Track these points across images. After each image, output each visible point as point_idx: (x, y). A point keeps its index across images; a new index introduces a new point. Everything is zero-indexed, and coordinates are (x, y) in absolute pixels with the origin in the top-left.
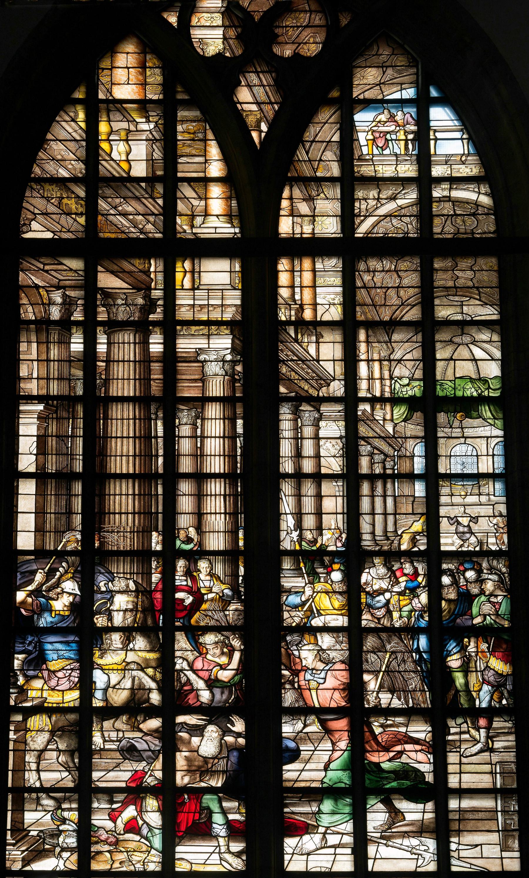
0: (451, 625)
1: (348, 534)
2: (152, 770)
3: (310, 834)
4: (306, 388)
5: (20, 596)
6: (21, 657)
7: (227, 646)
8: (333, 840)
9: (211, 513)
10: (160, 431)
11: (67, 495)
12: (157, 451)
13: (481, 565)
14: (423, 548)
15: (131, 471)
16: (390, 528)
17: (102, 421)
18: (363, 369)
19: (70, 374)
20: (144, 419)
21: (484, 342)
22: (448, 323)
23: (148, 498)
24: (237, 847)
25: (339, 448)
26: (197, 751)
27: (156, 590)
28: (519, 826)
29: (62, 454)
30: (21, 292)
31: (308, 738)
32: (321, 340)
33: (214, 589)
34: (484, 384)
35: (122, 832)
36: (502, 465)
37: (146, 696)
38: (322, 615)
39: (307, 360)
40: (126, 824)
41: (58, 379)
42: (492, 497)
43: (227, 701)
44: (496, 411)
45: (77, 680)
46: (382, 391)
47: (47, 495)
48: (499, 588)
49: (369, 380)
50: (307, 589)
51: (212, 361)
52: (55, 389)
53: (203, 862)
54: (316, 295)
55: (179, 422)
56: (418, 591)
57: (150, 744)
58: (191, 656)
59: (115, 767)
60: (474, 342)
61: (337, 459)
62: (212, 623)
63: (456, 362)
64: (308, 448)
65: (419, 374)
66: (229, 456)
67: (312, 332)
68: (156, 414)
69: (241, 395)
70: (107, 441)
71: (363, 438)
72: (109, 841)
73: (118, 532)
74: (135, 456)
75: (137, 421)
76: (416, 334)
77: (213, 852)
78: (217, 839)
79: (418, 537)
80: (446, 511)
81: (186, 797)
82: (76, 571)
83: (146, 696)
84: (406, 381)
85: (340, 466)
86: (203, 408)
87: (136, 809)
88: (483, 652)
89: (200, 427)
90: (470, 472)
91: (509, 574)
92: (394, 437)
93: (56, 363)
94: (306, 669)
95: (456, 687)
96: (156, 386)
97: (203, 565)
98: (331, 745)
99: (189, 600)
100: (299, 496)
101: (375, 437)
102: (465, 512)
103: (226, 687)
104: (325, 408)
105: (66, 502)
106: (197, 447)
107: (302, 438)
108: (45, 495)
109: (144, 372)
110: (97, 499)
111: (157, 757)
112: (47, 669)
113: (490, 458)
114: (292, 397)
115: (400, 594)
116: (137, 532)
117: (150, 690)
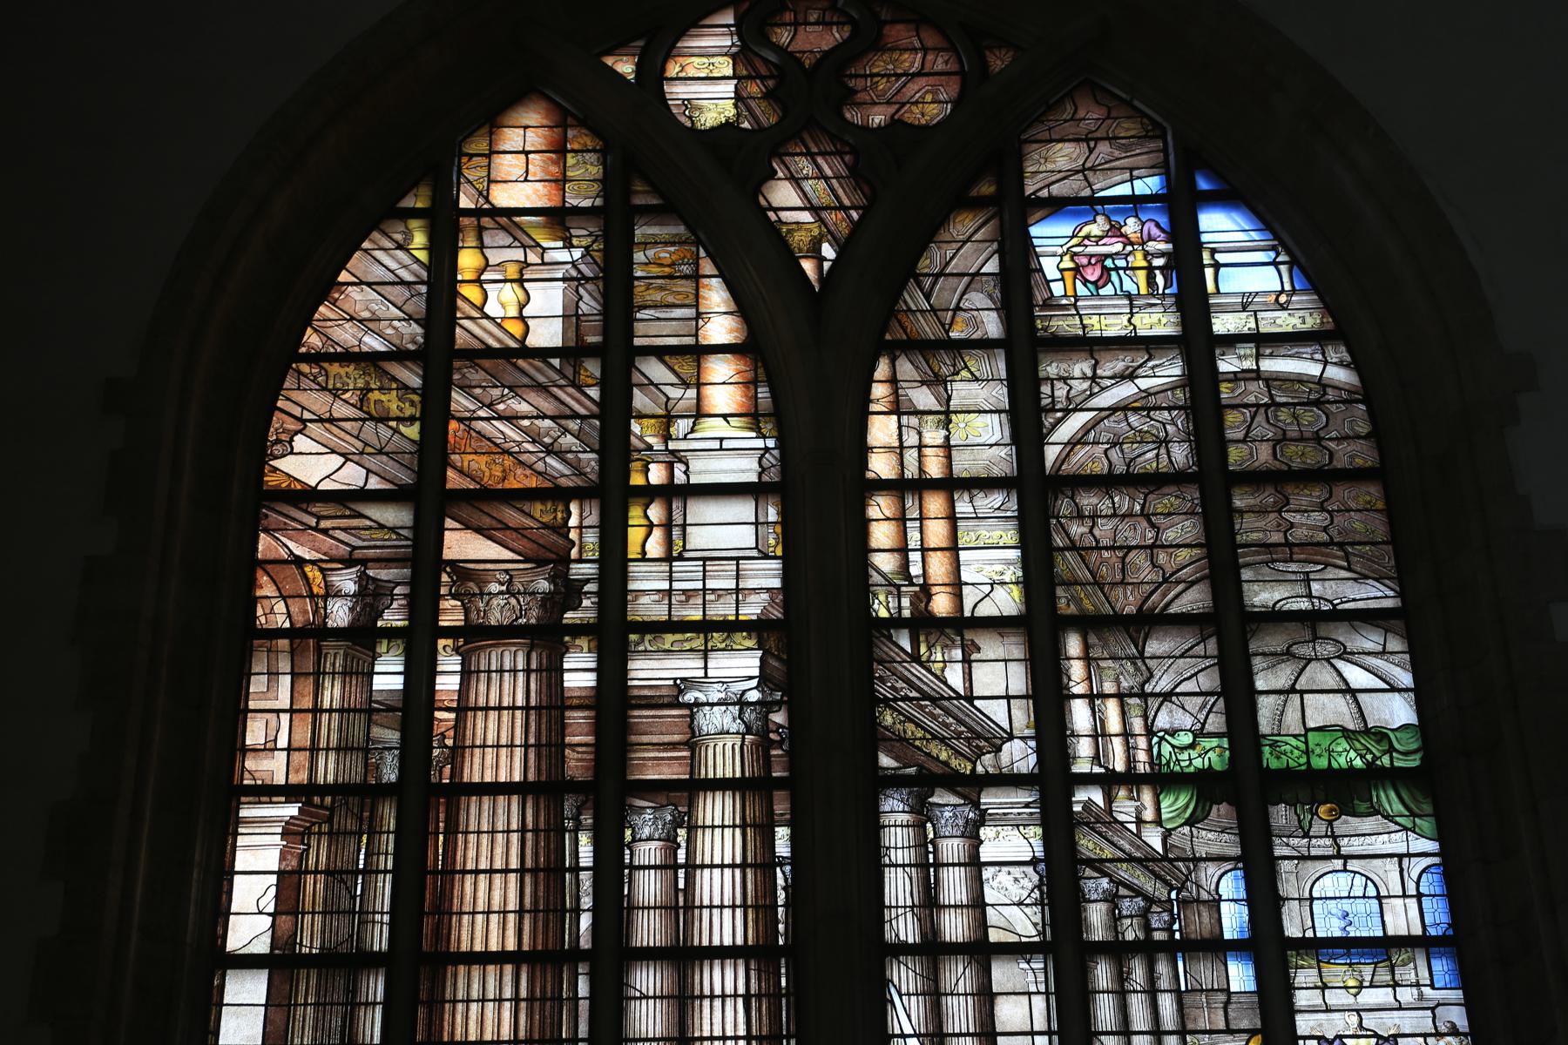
4: (943, 756)
10: (586, 855)
11: (346, 1004)
12: (578, 899)
15: (511, 945)
17: (441, 837)
18: (1080, 716)
19: (368, 739)
20: (547, 831)
21: (1369, 654)
22: (1275, 617)
23: (552, 1007)
25: (1030, 886)
29: (338, 912)
32: (975, 656)
34: (1378, 742)
36: (1444, 918)
39: (943, 698)
42: (1427, 991)
44: (1414, 799)
46: (1130, 760)
47: (296, 1005)
49: (1095, 736)
51: (712, 705)
54: (958, 566)
55: (633, 835)
60: (1345, 655)
61: (1027, 910)
63: (1306, 696)
64: (954, 886)
65: (1216, 722)
66: (756, 907)
67: (953, 641)
68: (576, 819)
69: (785, 774)
70: (453, 880)
71: (1090, 863)
74: (521, 912)
75: (529, 835)
76: (1203, 640)
80: (1311, 1023)
84: (1186, 739)
85: (1035, 925)
86: (692, 805)
89: (683, 844)
90: (1365, 934)
92: (1165, 858)
93: (335, 716)
96: (578, 760)
100: (934, 995)
101: (1120, 860)
102: (1360, 1025)
104: (989, 799)
105: (344, 1021)
106: (677, 889)
107: (938, 865)
108: (289, 1005)
109: (549, 730)
110: (421, 1013)
113: (1412, 903)
114: (909, 776)
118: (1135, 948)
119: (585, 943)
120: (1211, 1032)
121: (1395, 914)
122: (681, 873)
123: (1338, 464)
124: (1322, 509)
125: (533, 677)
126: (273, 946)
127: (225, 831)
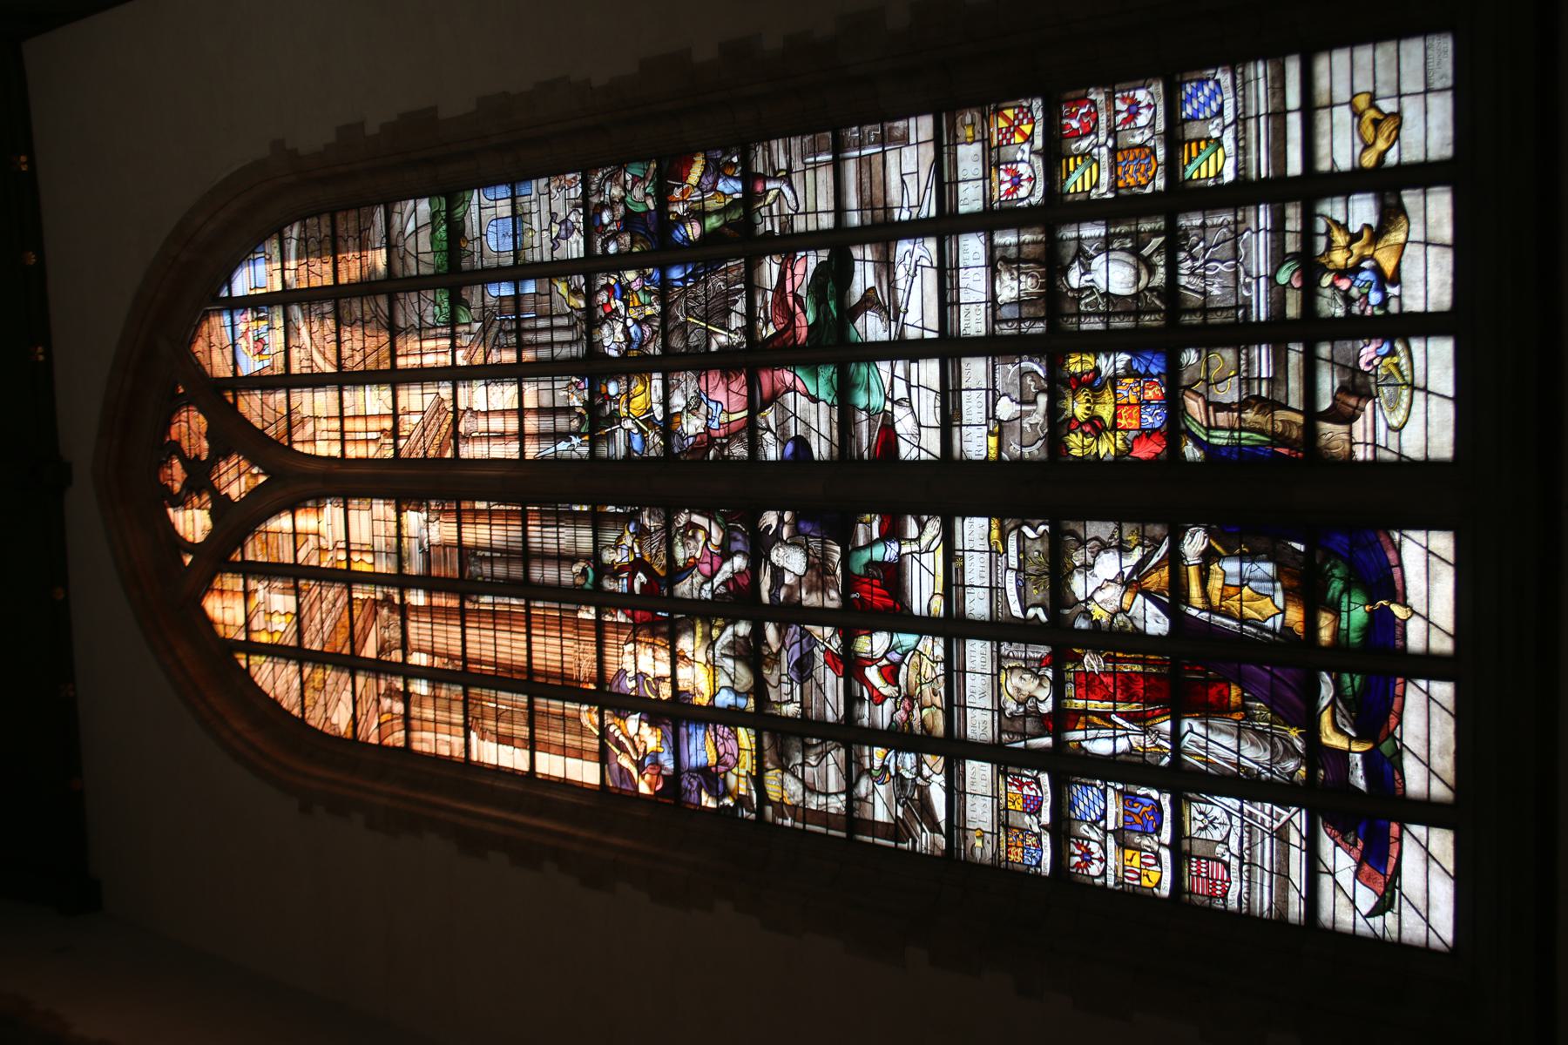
0: (656, 239)
1: (572, 375)
2: (824, 640)
3: (893, 424)
4: (446, 426)
5: (644, 789)
6: (704, 797)
7: (686, 531)
8: (900, 391)
9: (558, 544)
13: (597, 205)
14: (583, 281)
16: (564, 322)
24: (912, 529)
26: (801, 577)
27: (633, 618)
28: (876, 123)
30: (386, 742)
31: (782, 424)
33: (630, 545)
35: (897, 688)
37: (741, 640)
38: (651, 407)
40: (888, 683)
41: (450, 712)
42: (533, 197)
43: (743, 534)
45: (726, 729)
48: (617, 179)
50: (626, 427)
52: (458, 718)
53: (932, 577)
56: (624, 283)
57: (794, 640)
58: (699, 579)
59: (821, 689)
60: (402, 232)
62: (663, 548)
63: (419, 251)
64: (497, 424)
65: (430, 295)
72: (907, 707)
73: (580, 660)
75: (482, 625)
76: (398, 299)
77: (919, 561)
78: (904, 555)
79: (573, 287)
81: (853, 596)
82: (618, 716)
83: (741, 640)
84: (437, 308)
87: (870, 666)
88: (683, 194)
91: (604, 167)
92: (483, 322)
94: (707, 427)
95: (721, 226)
97: (608, 556)
98: (789, 394)
99: (641, 578)
103: (729, 534)
104: (462, 405)
111: (809, 632)
112: (716, 766)
113: (499, 203)
115: (627, 308)
116: (579, 636)
117: (735, 635)
118: (519, 338)
119: (522, 602)
120: (551, 303)
121: (503, 212)
122: (495, 555)
123: (330, 233)
124: (347, 241)
125: (421, 619)
126: (525, 748)
127: (481, 768)
